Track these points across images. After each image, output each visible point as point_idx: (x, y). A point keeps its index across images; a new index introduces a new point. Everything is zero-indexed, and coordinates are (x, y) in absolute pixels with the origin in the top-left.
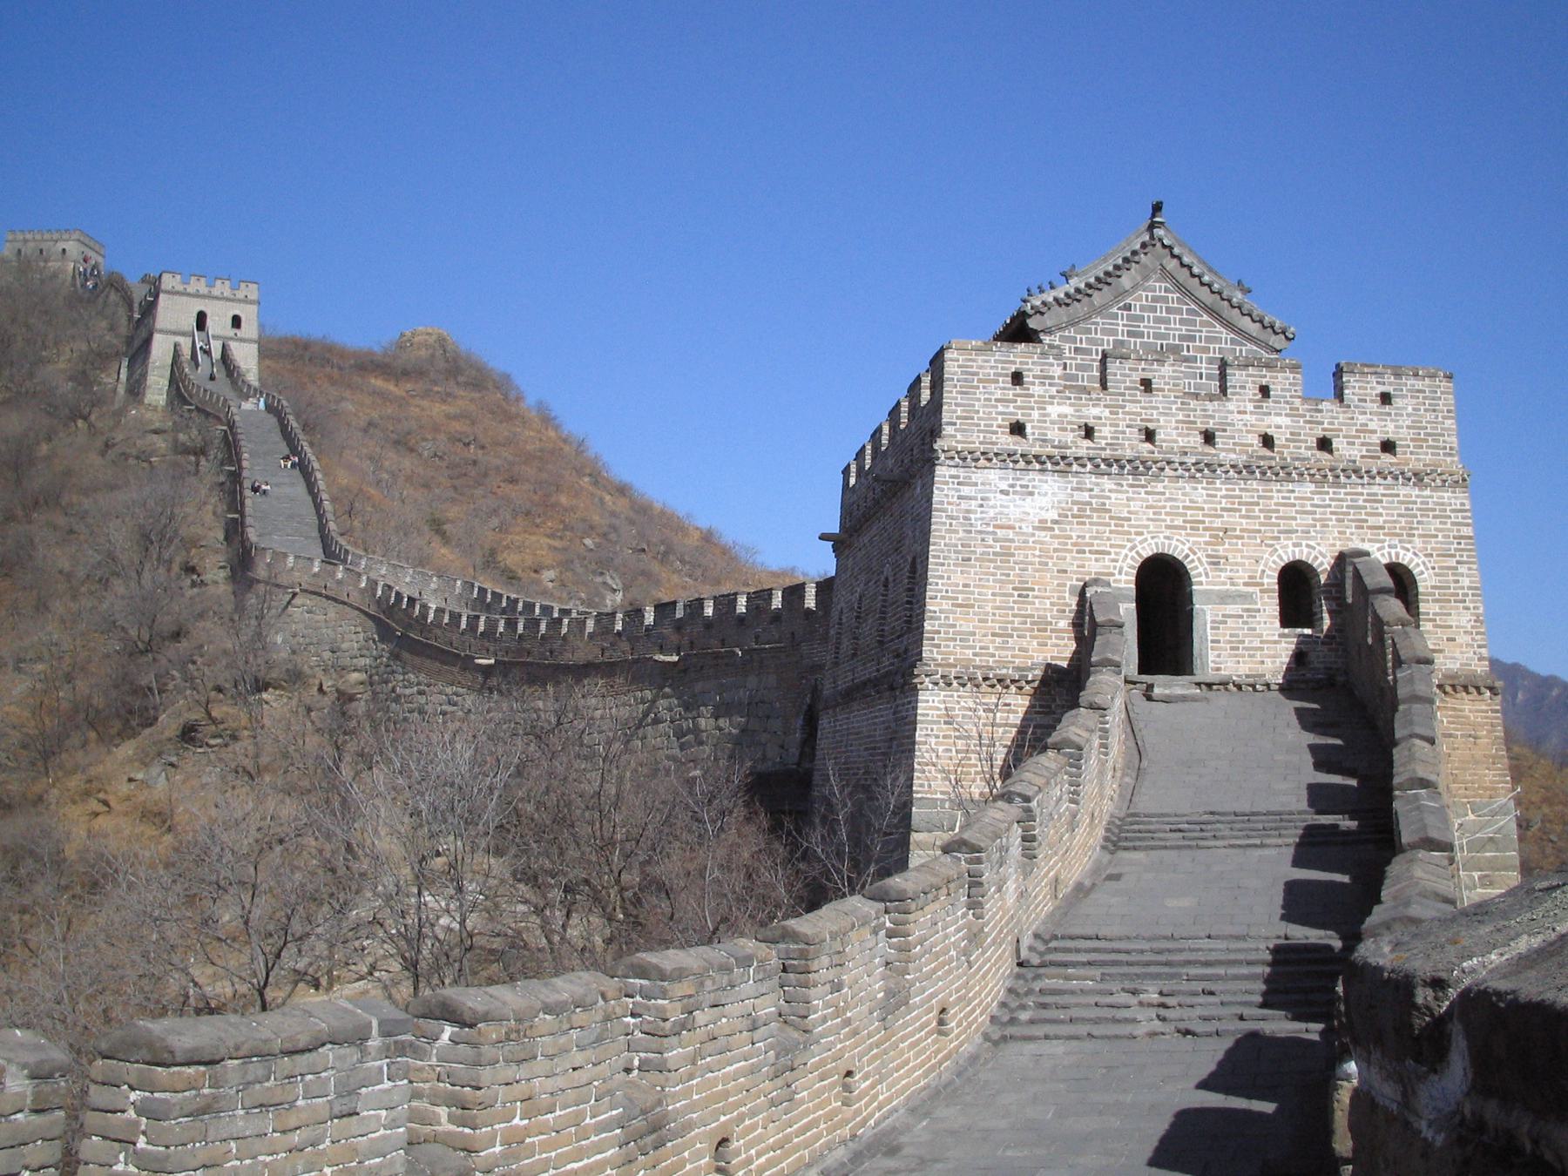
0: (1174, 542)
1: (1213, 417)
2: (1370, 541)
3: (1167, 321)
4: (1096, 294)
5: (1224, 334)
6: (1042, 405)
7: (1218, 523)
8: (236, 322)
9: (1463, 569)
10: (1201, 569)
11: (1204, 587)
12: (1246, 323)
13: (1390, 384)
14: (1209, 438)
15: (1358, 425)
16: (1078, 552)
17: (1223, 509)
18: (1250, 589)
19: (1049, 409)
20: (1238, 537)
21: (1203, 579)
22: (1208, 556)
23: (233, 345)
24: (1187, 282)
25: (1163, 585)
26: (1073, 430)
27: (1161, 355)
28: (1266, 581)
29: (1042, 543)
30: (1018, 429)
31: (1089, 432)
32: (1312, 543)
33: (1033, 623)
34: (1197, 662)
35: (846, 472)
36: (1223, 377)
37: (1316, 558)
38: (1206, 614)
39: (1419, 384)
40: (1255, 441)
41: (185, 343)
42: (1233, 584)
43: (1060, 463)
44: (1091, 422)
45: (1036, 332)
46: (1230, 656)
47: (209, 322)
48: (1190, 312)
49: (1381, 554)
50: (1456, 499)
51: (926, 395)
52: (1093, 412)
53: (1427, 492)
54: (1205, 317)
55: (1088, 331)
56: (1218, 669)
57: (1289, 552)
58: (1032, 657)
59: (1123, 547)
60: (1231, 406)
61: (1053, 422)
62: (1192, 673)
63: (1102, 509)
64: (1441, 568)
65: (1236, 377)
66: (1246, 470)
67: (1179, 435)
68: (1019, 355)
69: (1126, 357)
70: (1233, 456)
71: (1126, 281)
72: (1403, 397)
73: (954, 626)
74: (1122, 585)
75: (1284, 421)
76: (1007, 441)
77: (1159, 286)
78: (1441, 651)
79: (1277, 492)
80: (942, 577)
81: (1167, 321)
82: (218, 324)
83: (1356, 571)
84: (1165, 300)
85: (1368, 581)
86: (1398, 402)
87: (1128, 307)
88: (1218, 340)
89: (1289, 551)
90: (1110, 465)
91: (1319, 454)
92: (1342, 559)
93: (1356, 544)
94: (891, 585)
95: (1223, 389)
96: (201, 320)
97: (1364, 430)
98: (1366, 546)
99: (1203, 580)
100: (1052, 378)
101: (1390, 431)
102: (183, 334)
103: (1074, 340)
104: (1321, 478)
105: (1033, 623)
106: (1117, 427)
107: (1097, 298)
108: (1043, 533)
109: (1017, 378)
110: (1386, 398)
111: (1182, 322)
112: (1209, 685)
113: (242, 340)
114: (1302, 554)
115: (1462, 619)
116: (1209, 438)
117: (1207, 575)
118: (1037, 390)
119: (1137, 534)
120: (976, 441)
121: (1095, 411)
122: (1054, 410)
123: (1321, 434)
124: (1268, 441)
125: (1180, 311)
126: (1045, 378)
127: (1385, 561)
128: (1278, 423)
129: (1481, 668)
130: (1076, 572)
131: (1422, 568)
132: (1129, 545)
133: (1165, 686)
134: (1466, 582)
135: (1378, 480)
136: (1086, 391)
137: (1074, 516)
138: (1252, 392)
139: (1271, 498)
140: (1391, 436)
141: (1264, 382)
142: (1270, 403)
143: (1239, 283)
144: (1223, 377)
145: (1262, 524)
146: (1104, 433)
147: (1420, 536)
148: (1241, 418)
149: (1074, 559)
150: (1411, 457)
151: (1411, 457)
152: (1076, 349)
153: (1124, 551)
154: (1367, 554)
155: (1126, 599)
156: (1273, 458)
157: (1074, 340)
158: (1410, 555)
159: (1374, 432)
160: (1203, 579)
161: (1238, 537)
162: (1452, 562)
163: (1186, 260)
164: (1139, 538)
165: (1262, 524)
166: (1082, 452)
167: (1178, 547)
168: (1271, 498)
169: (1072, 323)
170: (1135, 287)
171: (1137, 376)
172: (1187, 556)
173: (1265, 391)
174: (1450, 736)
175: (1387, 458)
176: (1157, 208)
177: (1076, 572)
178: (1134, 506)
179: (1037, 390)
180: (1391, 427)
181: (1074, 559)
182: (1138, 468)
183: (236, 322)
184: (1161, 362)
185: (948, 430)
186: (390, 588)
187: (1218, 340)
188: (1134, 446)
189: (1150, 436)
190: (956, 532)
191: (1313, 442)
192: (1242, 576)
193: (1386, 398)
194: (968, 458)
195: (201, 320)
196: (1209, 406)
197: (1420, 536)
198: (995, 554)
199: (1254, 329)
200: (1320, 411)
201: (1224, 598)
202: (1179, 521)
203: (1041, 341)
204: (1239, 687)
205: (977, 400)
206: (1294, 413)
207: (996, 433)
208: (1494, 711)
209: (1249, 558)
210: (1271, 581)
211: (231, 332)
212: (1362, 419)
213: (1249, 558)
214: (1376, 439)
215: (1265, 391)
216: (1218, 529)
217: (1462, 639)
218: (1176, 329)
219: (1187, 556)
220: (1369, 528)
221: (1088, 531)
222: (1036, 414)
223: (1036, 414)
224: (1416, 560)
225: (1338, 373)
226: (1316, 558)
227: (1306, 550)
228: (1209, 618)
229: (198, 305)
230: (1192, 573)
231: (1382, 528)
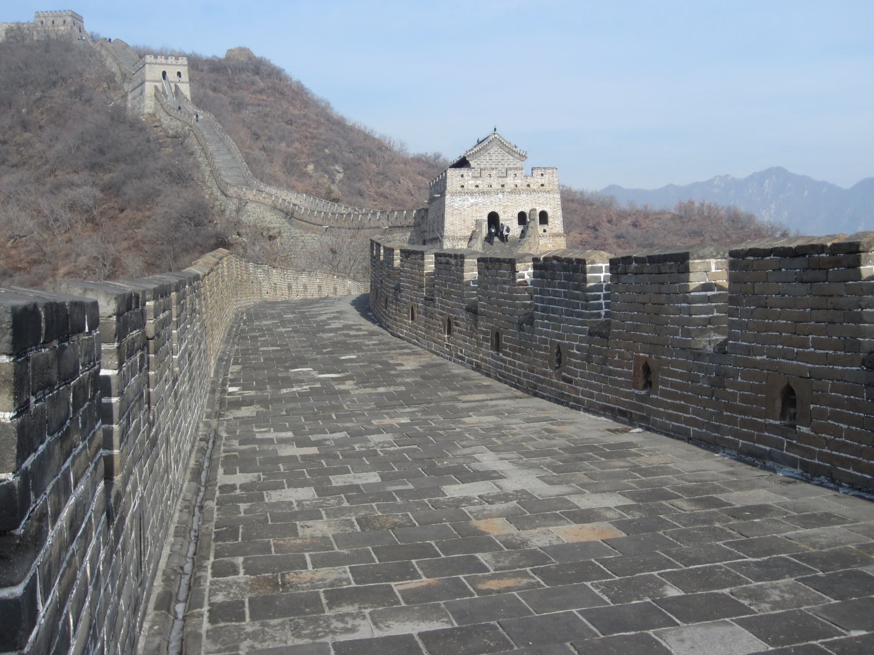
8: (179, 74)
12: (516, 155)
14: (503, 186)
23: (179, 85)
25: (493, 218)
27: (493, 169)
47: (168, 75)
52: (478, 182)
65: (509, 172)
66: (511, 192)
68: (464, 171)
71: (488, 147)
77: (496, 148)
82: (172, 75)
96: (164, 74)
102: (157, 81)
110: (542, 175)
113: (183, 82)
128: (518, 182)
138: (512, 175)
146: (481, 187)
148: (510, 181)
150: (547, 188)
151: (547, 188)
167: (496, 210)
183: (179, 74)
186: (285, 200)
188: (486, 188)
194: (453, 194)
195: (164, 74)
210: (516, 216)
211: (177, 79)
229: (163, 68)
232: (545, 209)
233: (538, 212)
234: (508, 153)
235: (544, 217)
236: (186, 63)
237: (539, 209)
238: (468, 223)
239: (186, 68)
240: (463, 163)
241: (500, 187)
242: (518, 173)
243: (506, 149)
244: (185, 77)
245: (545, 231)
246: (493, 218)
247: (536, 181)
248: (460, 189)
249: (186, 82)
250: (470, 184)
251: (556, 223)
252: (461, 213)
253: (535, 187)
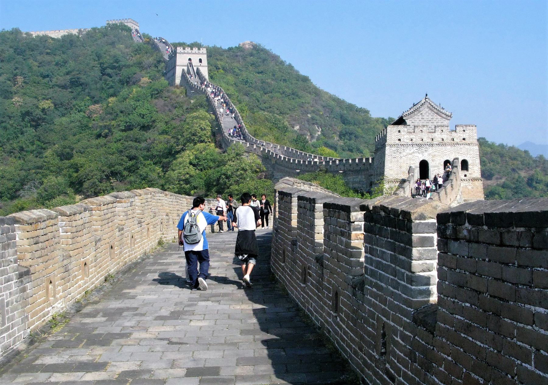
5: (439, 117)
6: (404, 135)
8: (200, 61)
23: (200, 68)
24: (432, 108)
27: (424, 126)
39: (471, 128)
40: (440, 139)
41: (186, 68)
68: (400, 127)
71: (421, 109)
75: (445, 136)
77: (427, 110)
82: (195, 62)
93: (457, 156)
96: (190, 59)
99: (431, 164)
104: (451, 145)
120: (392, 143)
128: (444, 136)
138: (440, 131)
146: (414, 140)
148: (438, 136)
150: (467, 141)
163: (432, 104)
176: (426, 95)
179: (402, 133)
183: (200, 61)
185: (388, 141)
193: (464, 131)
194: (391, 146)
195: (190, 59)
199: (445, 116)
201: (434, 167)
211: (199, 64)
214: (462, 138)
232: (466, 159)
233: (460, 160)
234: (437, 113)
235: (465, 165)
236: (206, 52)
239: (206, 56)
240: (401, 121)
242: (445, 129)
243: (435, 110)
244: (205, 62)
245: (465, 176)
247: (458, 136)
248: (398, 142)
249: (205, 66)
251: (475, 170)
252: (398, 161)
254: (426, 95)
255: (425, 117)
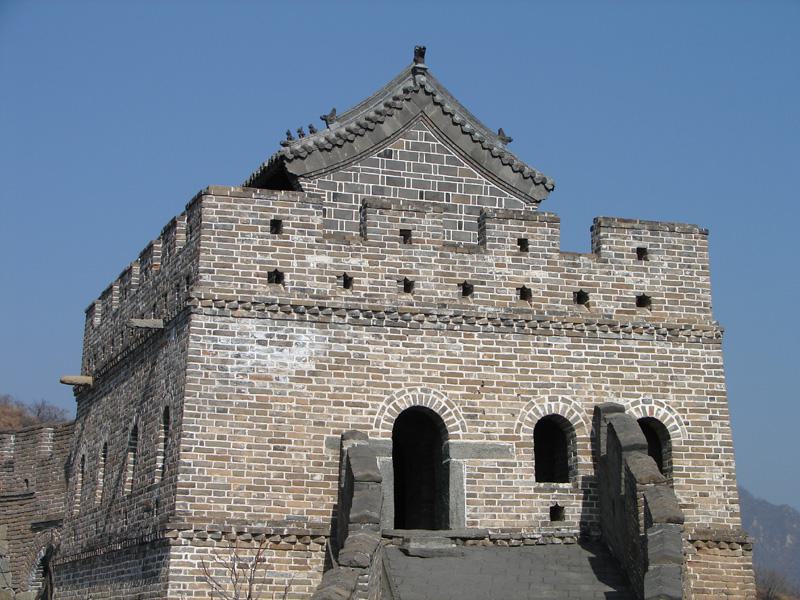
0: (432, 395)
1: (471, 270)
2: (624, 395)
3: (427, 169)
4: (358, 140)
7: (475, 376)
9: (715, 425)
10: (458, 423)
11: (461, 440)
12: (506, 173)
13: (647, 239)
14: (467, 289)
15: (615, 281)
16: (336, 404)
17: (480, 362)
18: (506, 443)
19: (309, 258)
20: (494, 391)
21: (460, 432)
22: (465, 409)
25: (420, 438)
26: (332, 281)
28: (522, 434)
29: (299, 394)
30: (276, 277)
31: (348, 282)
32: (567, 397)
33: (288, 476)
34: (453, 516)
35: (90, 311)
36: (482, 229)
37: (572, 412)
38: (462, 467)
39: (675, 240)
40: (514, 295)
42: (489, 438)
43: (317, 313)
44: (350, 272)
45: (295, 177)
46: (486, 510)
48: (451, 160)
49: (635, 409)
50: (708, 355)
51: (181, 238)
53: (681, 348)
54: (466, 166)
55: (347, 177)
56: (475, 523)
57: (545, 406)
58: (288, 511)
59: (381, 399)
60: (489, 259)
61: (311, 272)
62: (447, 528)
63: (360, 361)
64: (694, 423)
65: (495, 230)
66: (504, 323)
67: (438, 287)
68: (278, 203)
69: (385, 207)
70: (491, 309)
71: (387, 128)
72: (658, 252)
73: (209, 479)
74: (379, 438)
76: (263, 290)
78: (693, 507)
79: (534, 346)
80: (197, 429)
81: (427, 169)
83: (610, 426)
84: (426, 147)
85: (621, 436)
86: (654, 258)
87: (388, 154)
88: (477, 189)
89: (546, 405)
90: (369, 316)
91: (576, 308)
92: (598, 413)
93: (611, 399)
94: (140, 436)
95: (482, 241)
97: (621, 285)
98: (621, 401)
99: (460, 433)
100: (313, 227)
101: (645, 285)
103: (333, 186)
105: (288, 476)
106: (375, 279)
107: (359, 145)
108: (301, 385)
109: (276, 226)
110: (642, 253)
111: (442, 170)
112: (464, 539)
114: (558, 408)
115: (715, 475)
116: (467, 289)
117: (464, 430)
118: (296, 238)
119: (394, 386)
120: (234, 289)
121: (354, 262)
122: (313, 260)
123: (578, 288)
124: (525, 294)
125: (439, 159)
126: (305, 227)
127: (639, 416)
128: (537, 276)
129: (732, 523)
130: (333, 425)
131: (675, 423)
132: (387, 397)
133: (421, 541)
134: (718, 437)
135: (633, 335)
136: (343, 239)
137: (331, 368)
138: (511, 245)
139: (528, 351)
140: (646, 291)
141: (523, 235)
142: (527, 257)
143: (500, 131)
144: (482, 229)
145: (518, 378)
147: (674, 391)
148: (499, 270)
149: (332, 411)
150: (665, 313)
151: (665, 313)
152: (335, 196)
153: (382, 404)
154: (621, 409)
155: (383, 452)
156: (530, 312)
157: (333, 186)
158: (663, 410)
159: (630, 287)
160: (460, 432)
161: (494, 391)
162: (705, 418)
164: (397, 391)
165: (518, 378)
166: (341, 303)
167: (436, 400)
168: (528, 351)
169: (332, 169)
170: (396, 134)
171: (397, 227)
172: (444, 409)
173: (523, 244)
174: (703, 591)
175: (644, 313)
176: (420, 53)
177: (333, 425)
178: (393, 358)
180: (647, 281)
181: (332, 411)
182: (396, 320)
184: (421, 213)
185: (206, 278)
187: (477, 189)
188: (390, 297)
189: (408, 286)
190: (213, 382)
191: (569, 296)
192: (499, 429)
194: (224, 307)
196: (470, 259)
197: (674, 391)
198: (251, 405)
200: (578, 265)
201: (481, 452)
202: (436, 374)
203: (299, 188)
204: (494, 540)
205: (237, 242)
206: (551, 267)
207: (255, 281)
208: (749, 567)
209: (505, 411)
210: (527, 434)
212: (618, 274)
213: (507, 411)
214: (632, 294)
215: (523, 244)
216: (475, 382)
217: (715, 494)
218: (436, 177)
219: (444, 409)
220: (623, 382)
221: (346, 383)
222: (295, 263)
223: (295, 263)
224: (670, 415)
225: (596, 228)
226: (572, 412)
227: (562, 404)
228: (465, 472)
230: (449, 426)
231: (638, 383)
237: (636, 412)
238: (298, 457)
241: (454, 292)
246: (420, 438)
250: (313, 266)
253: (612, 308)
254: (420, 53)
255: (408, 175)
